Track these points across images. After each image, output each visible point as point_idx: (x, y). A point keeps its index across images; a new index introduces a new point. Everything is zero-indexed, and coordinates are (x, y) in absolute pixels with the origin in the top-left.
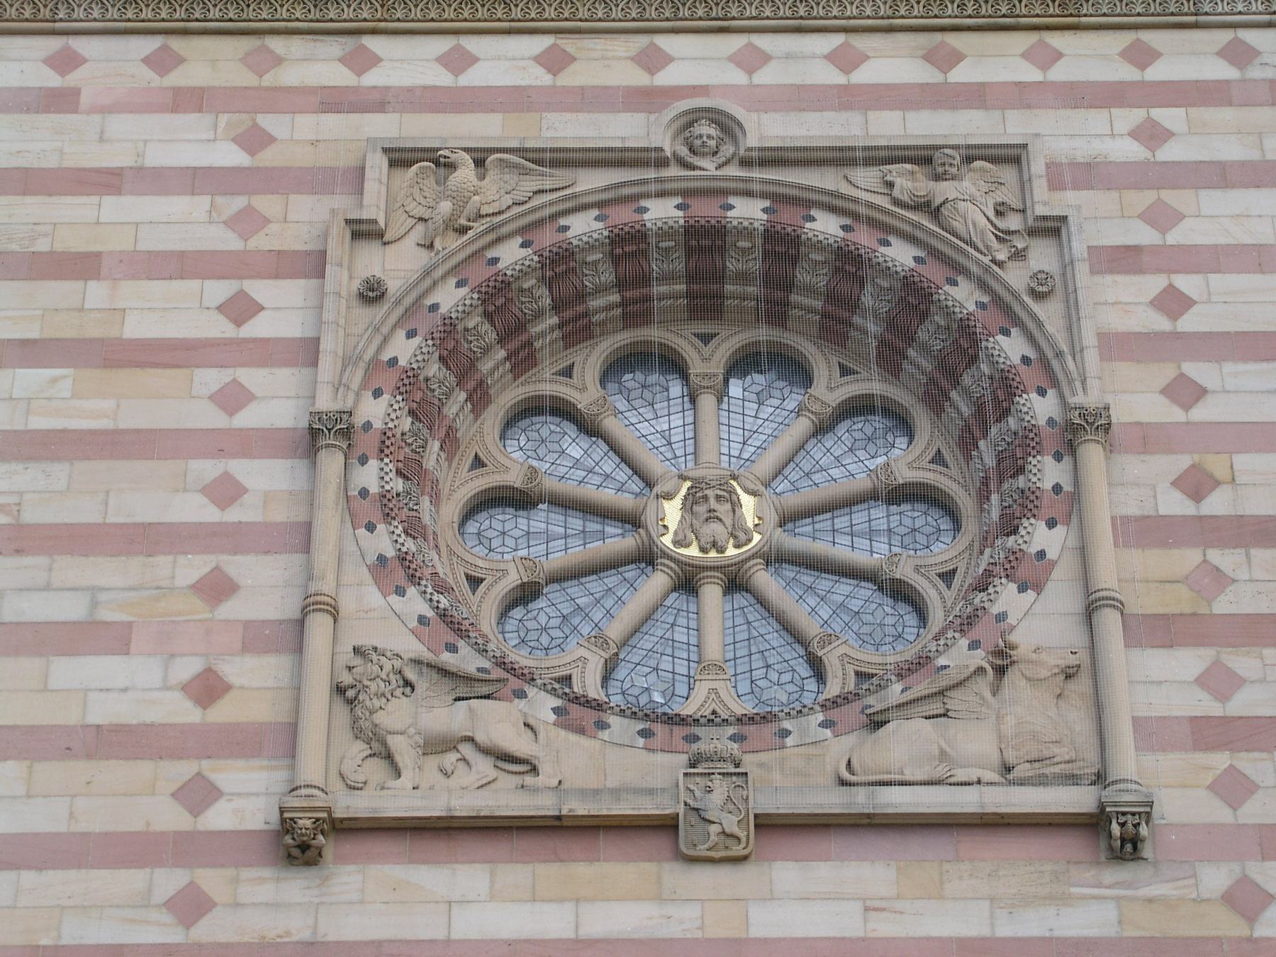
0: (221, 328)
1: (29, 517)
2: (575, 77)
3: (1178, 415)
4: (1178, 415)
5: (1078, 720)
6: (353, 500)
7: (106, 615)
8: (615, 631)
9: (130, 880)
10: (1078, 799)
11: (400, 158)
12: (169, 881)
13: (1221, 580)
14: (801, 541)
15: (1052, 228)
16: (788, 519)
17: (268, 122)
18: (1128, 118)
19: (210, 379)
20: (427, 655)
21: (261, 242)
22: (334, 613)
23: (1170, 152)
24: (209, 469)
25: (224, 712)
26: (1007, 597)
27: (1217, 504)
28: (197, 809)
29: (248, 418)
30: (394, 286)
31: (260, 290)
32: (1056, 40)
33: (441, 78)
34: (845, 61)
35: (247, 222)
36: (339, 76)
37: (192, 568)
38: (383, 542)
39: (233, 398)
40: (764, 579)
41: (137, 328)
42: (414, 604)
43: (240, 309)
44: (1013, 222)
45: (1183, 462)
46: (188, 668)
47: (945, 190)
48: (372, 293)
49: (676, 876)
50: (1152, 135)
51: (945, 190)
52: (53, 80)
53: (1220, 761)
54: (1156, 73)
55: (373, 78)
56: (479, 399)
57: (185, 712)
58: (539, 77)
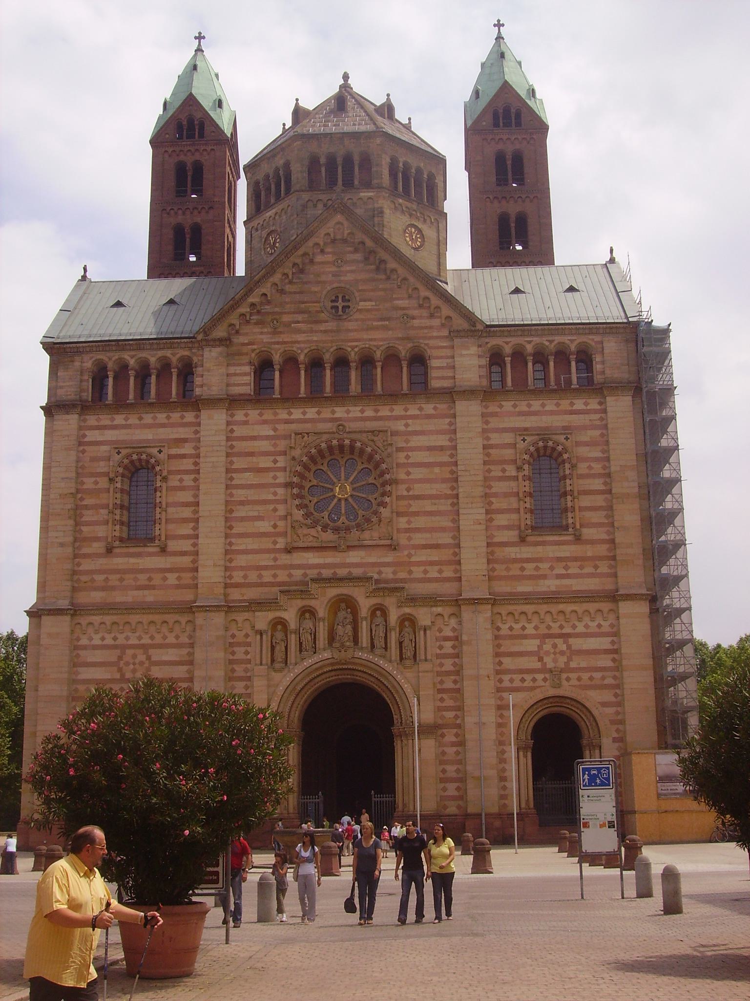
0: (272, 465)
1: (249, 499)
2: (323, 416)
3: (406, 477)
4: (406, 477)
5: (389, 528)
6: (293, 495)
7: (261, 515)
8: (330, 508)
9: (267, 556)
10: (388, 542)
11: (296, 434)
12: (272, 556)
13: (411, 505)
14: (354, 493)
15: (391, 445)
16: (354, 489)
17: (277, 426)
18: (403, 422)
19: (272, 474)
20: (305, 522)
21: (278, 449)
22: (291, 515)
23: (410, 429)
24: (272, 490)
25: (278, 530)
26: (382, 509)
27: (411, 493)
28: (275, 545)
29: (277, 481)
30: (296, 457)
31: (278, 458)
32: (394, 407)
33: (302, 417)
34: (362, 411)
35: (275, 445)
36: (285, 416)
37: (271, 507)
38: (297, 502)
39: (275, 477)
40: (350, 500)
41: (262, 465)
42: (302, 512)
43: (275, 461)
44: (385, 443)
45: (407, 486)
46: (272, 523)
47: (375, 439)
48: (294, 459)
49: (337, 554)
50: (407, 425)
51: (375, 439)
52: (244, 419)
53: (408, 534)
54: (408, 413)
55: (292, 417)
56: (309, 470)
57: (272, 530)
58: (316, 416)
